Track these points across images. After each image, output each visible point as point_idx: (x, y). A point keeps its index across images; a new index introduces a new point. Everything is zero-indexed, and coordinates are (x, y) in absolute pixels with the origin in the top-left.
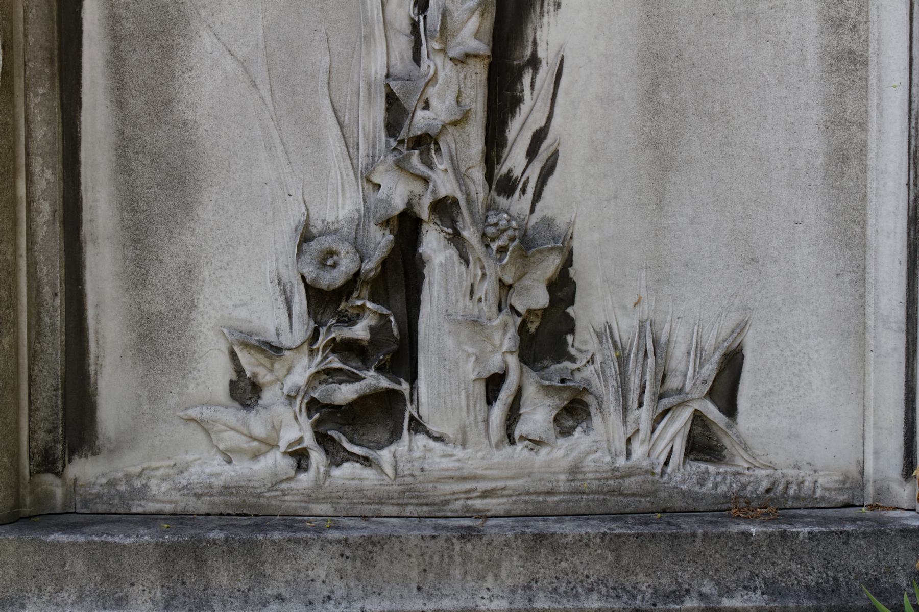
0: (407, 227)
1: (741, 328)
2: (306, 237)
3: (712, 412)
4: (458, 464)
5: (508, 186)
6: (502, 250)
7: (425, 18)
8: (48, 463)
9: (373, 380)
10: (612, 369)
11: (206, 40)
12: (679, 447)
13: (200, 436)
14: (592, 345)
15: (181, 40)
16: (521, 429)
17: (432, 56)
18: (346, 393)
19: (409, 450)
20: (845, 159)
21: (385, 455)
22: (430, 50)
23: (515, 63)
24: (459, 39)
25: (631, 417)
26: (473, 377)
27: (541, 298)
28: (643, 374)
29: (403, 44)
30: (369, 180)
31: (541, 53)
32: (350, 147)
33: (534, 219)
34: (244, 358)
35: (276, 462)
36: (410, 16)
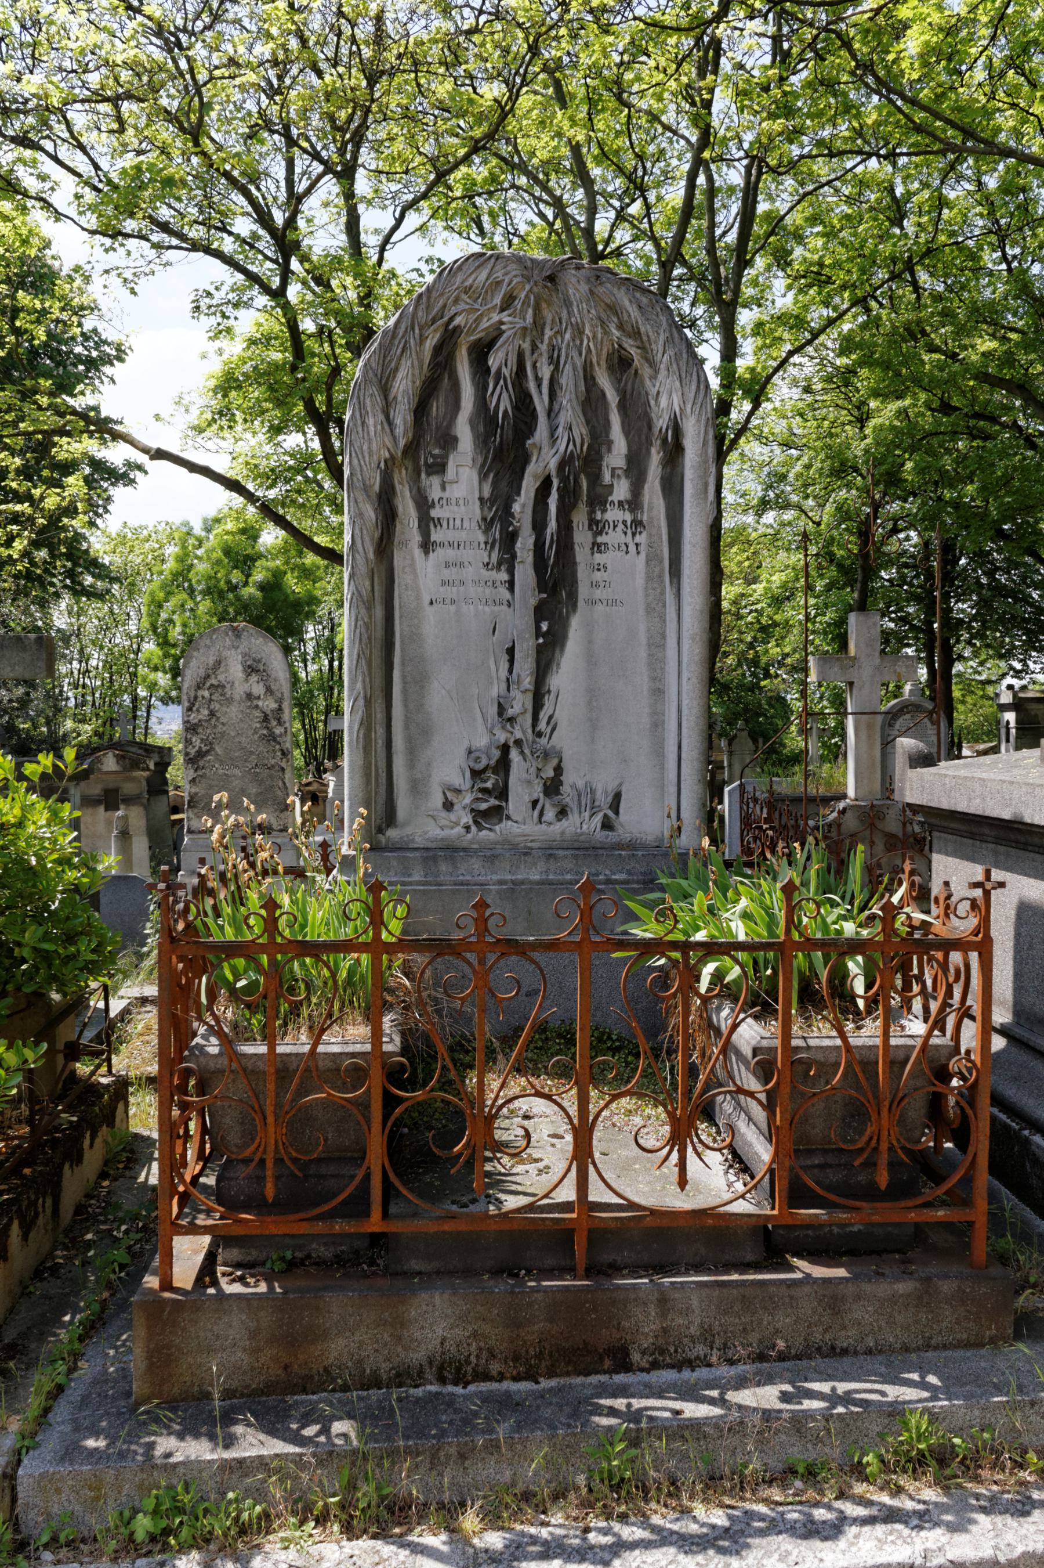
0: (505, 749)
2: (470, 752)
3: (610, 814)
5: (539, 735)
9: (493, 802)
11: (436, 684)
18: (484, 806)
19: (505, 826)
29: (504, 685)
32: (485, 720)
34: (449, 794)
35: (459, 830)
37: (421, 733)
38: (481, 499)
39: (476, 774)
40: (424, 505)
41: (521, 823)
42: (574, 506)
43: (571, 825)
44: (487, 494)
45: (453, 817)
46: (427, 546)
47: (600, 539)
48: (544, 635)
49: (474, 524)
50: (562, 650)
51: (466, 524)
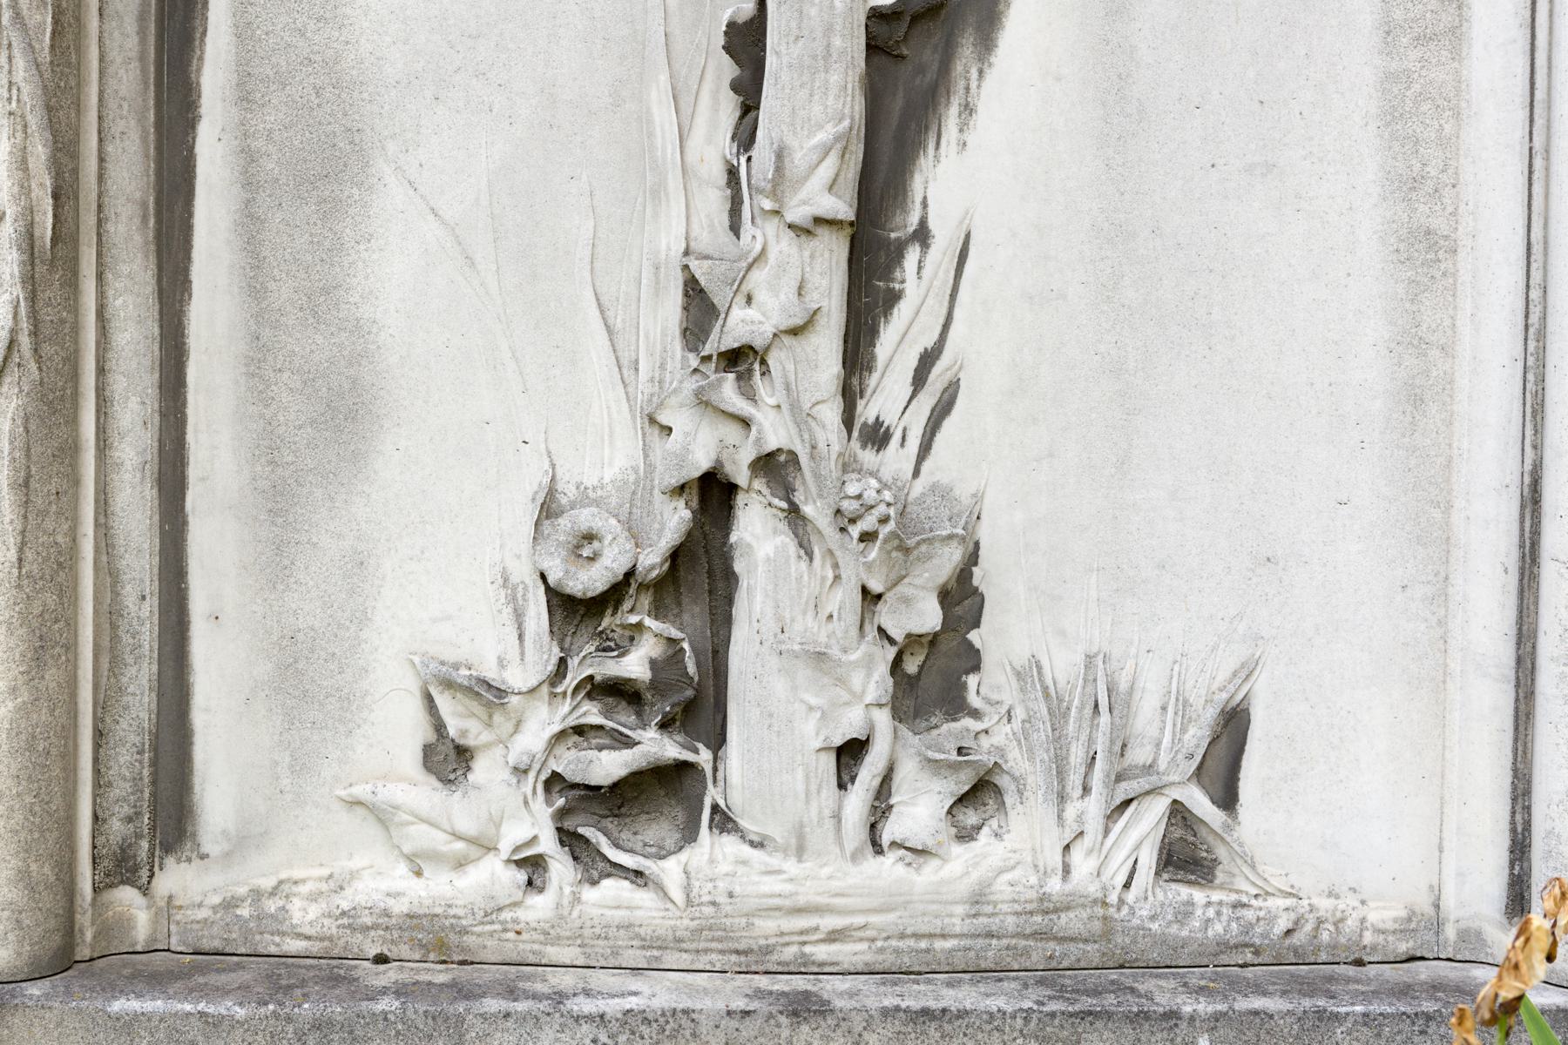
0: (713, 494)
1: (1247, 671)
2: (549, 509)
3: (1200, 803)
4: (788, 888)
5: (877, 436)
6: (867, 537)
7: (749, 159)
8: (122, 868)
9: (657, 745)
10: (1042, 733)
12: (1148, 859)
13: (372, 830)
14: (1008, 694)
15: (355, 191)
17: (758, 221)
18: (608, 766)
19: (712, 853)
20: (1417, 401)
21: (670, 870)
22: (756, 211)
23: (893, 235)
24: (803, 194)
25: (1071, 811)
26: (818, 745)
27: (929, 617)
28: (1091, 740)
29: (714, 201)
30: (652, 420)
31: (932, 224)
32: (626, 368)
33: (918, 488)
34: (444, 702)
35: (493, 876)
36: (725, 157)
37: (327, 417)
39: (573, 612)
41: (784, 854)
43: (1015, 858)
45: (461, 810)
50: (986, 44)
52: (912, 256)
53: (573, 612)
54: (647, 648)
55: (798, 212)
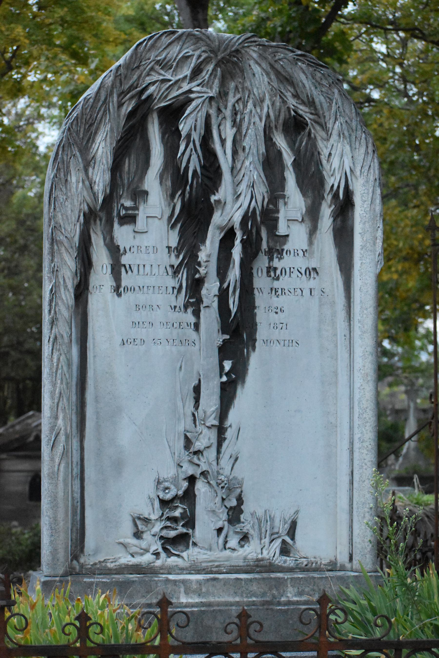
0: (192, 480)
1: (297, 512)
2: (159, 482)
3: (288, 539)
4: (208, 557)
6: (223, 487)
9: (181, 530)
14: (249, 519)
16: (228, 546)
18: (172, 534)
21: (185, 554)
26: (214, 528)
27: (234, 503)
28: (266, 527)
30: (179, 465)
34: (138, 522)
38: (169, 248)
39: (164, 503)
40: (115, 252)
42: (255, 255)
43: (251, 551)
44: (174, 243)
45: (144, 544)
46: (117, 290)
47: (276, 284)
48: (227, 374)
49: (162, 269)
51: (155, 270)
52: (229, 430)
53: (164, 503)
54: (178, 510)
55: (208, 424)
